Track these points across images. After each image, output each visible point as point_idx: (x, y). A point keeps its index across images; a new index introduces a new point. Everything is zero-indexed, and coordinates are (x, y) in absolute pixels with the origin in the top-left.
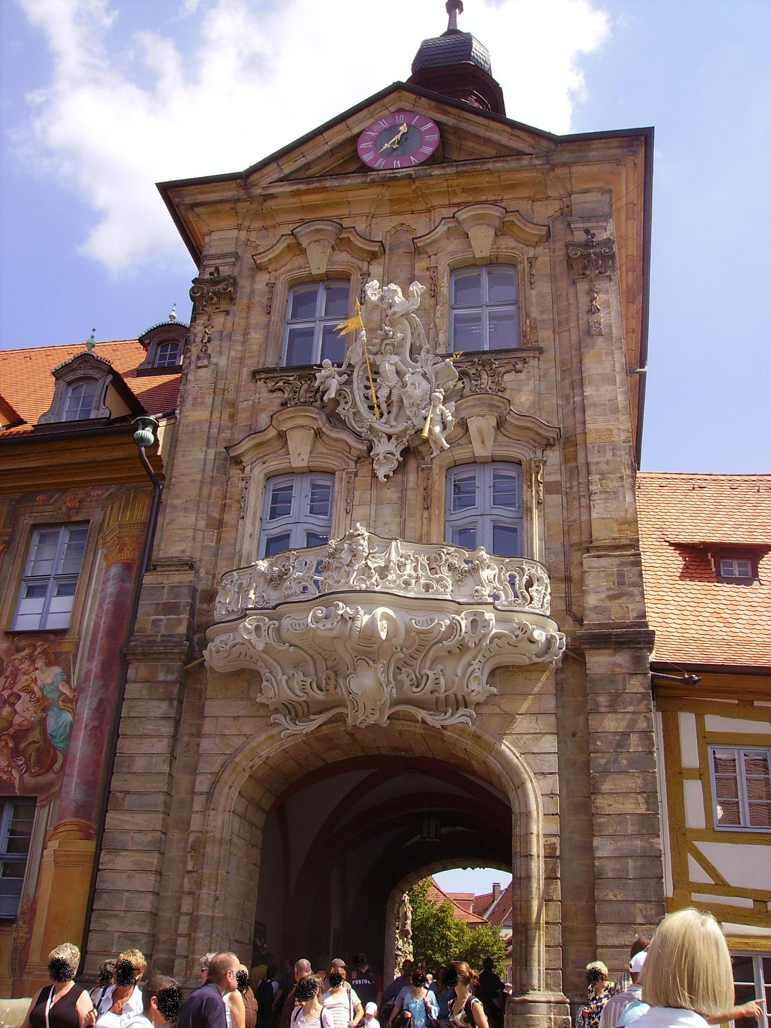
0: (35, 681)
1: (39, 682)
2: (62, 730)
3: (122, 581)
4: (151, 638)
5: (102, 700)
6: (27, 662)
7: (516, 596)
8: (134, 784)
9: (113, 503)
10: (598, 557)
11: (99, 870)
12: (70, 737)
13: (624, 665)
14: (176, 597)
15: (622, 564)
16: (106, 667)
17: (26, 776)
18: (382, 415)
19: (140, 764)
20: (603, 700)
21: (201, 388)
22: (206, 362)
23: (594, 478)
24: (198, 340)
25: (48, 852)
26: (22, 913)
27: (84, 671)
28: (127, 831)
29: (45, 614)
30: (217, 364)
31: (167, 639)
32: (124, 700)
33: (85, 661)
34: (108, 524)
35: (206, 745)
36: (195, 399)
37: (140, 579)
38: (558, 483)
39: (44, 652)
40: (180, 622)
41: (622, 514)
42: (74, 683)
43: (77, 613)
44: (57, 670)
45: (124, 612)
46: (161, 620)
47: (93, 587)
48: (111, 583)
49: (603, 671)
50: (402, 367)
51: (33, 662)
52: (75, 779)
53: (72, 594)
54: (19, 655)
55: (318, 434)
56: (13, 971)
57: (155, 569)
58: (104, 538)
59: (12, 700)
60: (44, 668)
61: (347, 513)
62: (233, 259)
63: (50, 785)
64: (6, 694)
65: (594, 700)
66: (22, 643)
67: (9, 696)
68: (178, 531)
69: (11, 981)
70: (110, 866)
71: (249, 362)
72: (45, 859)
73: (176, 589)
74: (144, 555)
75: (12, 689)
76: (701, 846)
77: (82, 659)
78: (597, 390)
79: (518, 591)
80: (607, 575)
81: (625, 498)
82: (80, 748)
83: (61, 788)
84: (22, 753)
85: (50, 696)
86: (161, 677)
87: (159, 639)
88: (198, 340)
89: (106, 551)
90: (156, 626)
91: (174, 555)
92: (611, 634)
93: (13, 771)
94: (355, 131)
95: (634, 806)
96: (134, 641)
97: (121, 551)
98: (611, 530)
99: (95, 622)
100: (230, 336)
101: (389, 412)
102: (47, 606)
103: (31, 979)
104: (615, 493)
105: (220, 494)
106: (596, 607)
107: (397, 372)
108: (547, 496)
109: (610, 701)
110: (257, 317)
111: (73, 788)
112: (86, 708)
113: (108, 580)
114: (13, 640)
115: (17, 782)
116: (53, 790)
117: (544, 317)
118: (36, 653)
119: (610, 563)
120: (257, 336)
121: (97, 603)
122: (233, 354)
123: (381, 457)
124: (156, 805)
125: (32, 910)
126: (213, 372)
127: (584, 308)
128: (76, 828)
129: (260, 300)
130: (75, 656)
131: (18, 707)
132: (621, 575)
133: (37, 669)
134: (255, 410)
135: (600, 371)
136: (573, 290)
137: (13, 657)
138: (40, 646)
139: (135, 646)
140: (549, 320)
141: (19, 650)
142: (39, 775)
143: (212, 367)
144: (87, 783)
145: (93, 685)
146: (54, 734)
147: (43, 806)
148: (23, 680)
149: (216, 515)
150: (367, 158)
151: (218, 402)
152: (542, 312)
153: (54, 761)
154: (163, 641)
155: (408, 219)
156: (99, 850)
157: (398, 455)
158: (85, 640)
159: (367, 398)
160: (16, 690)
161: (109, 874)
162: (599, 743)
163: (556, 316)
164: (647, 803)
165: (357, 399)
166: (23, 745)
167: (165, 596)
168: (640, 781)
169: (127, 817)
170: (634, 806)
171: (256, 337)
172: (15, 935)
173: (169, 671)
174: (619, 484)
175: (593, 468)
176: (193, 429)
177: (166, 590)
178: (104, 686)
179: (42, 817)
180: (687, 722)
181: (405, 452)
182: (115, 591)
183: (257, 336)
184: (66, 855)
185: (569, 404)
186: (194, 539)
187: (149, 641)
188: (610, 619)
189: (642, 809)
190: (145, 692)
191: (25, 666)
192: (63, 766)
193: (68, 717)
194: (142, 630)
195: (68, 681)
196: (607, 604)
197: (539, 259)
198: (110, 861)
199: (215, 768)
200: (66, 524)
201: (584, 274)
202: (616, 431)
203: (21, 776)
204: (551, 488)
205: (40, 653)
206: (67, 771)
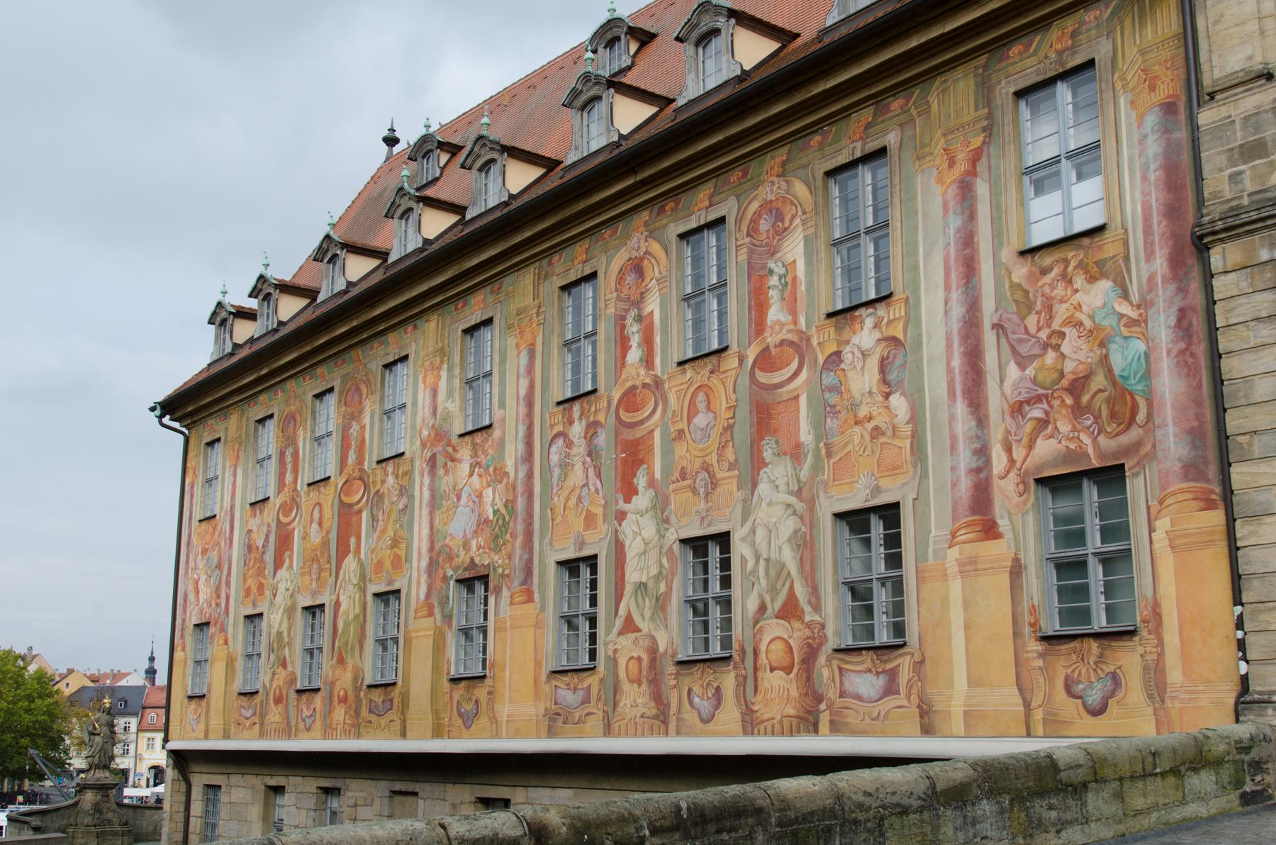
0: (1079, 307)
1: (1085, 308)
4: (1234, 204)
5: (1182, 313)
6: (1061, 286)
11: (1238, 549)
12: (1148, 374)
14: (1257, 130)
16: (1176, 262)
17: (1102, 439)
25: (1159, 535)
26: (1144, 621)
27: (1144, 280)
29: (1067, 211)
32: (1215, 302)
33: (1143, 263)
37: (1192, 119)
39: (1081, 266)
42: (1135, 297)
43: (1111, 197)
44: (1105, 285)
45: (1184, 174)
46: (1241, 173)
51: (1070, 282)
53: (1098, 173)
54: (1048, 279)
56: (1150, 697)
57: (1212, 98)
59: (1054, 341)
60: (1087, 286)
63: (1137, 445)
64: (1043, 335)
66: (1047, 259)
67: (1049, 337)
69: (1150, 710)
72: (1156, 546)
73: (1253, 119)
74: (1188, 80)
75: (1049, 326)
77: (1137, 260)
82: (1169, 385)
83: (1154, 446)
84: (1088, 408)
85: (1106, 323)
90: (1236, 183)
93: (1083, 437)
96: (1208, 214)
99: (1143, 203)
102: (1067, 199)
103: (1177, 705)
111: (1172, 443)
114: (1033, 261)
115: (1091, 451)
116: (1144, 451)
118: (1070, 269)
121: (1138, 175)
125: (1157, 614)
128: (1189, 496)
130: (1127, 258)
131: (1065, 348)
133: (1076, 291)
137: (1040, 284)
138: (1072, 255)
141: (1044, 272)
142: (1117, 435)
144: (1191, 432)
146: (1125, 374)
147: (1135, 475)
148: (1062, 312)
153: (1134, 410)
154: (1251, 204)
156: (1231, 520)
158: (1134, 233)
160: (1055, 326)
166: (1085, 399)
167: (1239, 134)
172: (1140, 650)
177: (1238, 126)
179: (1137, 489)
182: (1160, 150)
186: (1262, 33)
187: (1232, 209)
191: (1059, 291)
192: (1149, 417)
193: (1140, 346)
194: (1215, 195)
195: (1125, 296)
200: (1064, 76)
203: (1094, 440)
205: (1075, 268)
206: (1158, 421)
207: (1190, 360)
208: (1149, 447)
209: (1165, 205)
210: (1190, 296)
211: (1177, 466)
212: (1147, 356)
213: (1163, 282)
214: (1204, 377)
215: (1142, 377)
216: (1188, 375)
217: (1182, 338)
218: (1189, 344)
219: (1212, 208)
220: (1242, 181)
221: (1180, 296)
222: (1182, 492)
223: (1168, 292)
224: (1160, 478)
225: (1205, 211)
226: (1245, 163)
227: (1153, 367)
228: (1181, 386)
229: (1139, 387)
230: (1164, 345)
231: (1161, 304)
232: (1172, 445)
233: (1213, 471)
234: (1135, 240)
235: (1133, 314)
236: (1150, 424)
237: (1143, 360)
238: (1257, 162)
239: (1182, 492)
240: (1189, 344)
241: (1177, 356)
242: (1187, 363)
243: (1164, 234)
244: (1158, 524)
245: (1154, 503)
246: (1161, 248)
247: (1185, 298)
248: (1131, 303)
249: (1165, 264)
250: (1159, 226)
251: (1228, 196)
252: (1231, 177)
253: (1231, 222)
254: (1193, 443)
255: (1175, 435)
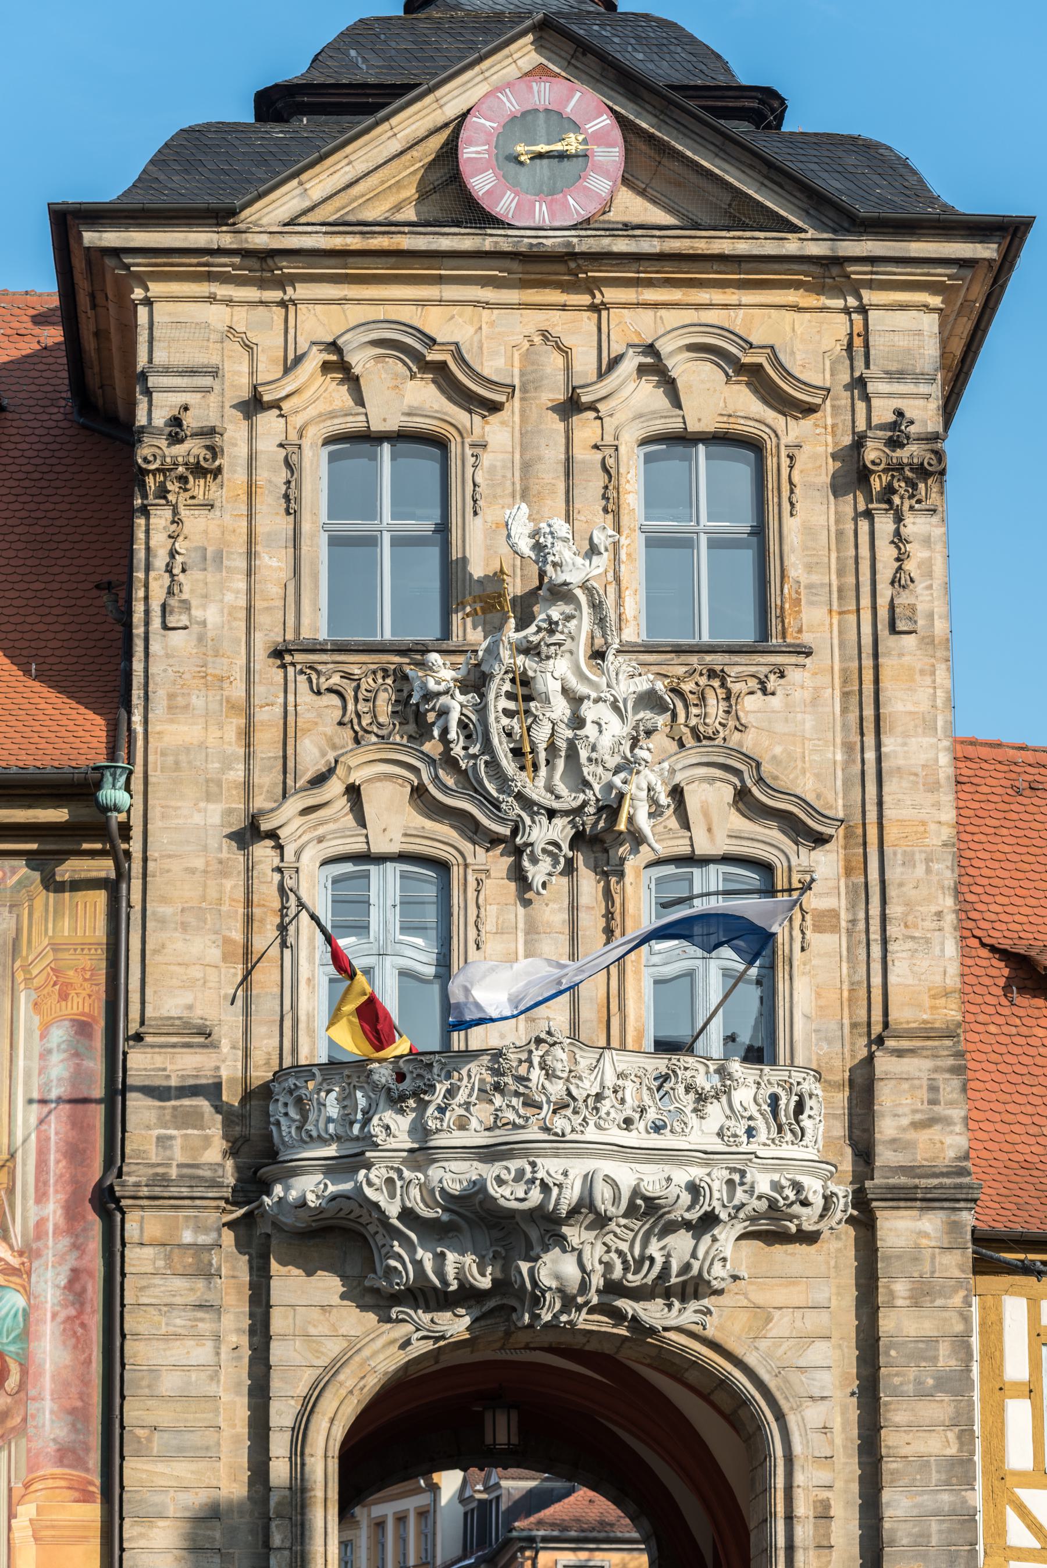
2: (9, 1321)
3: (77, 1054)
5: (76, 1273)
7: (780, 1129)
8: (163, 1415)
9: (31, 899)
10: (900, 1053)
12: (25, 1335)
13: (933, 1234)
15: (936, 1070)
16: (71, 1213)
18: (536, 767)
19: (169, 1383)
20: (901, 1288)
21: (181, 675)
22: (184, 620)
23: (894, 910)
24: (160, 561)
28: (164, 1489)
30: (204, 623)
31: (191, 1175)
34: (29, 942)
35: (278, 1352)
36: (171, 696)
38: (834, 914)
40: (207, 1140)
41: (938, 979)
42: (17, 1241)
46: (171, 1138)
47: (21, 1063)
48: (55, 1058)
49: (901, 1242)
50: (573, 682)
52: (48, 1404)
55: (419, 792)
58: (25, 969)
61: (478, 948)
62: (207, 381)
65: (888, 1287)
68: (177, 969)
70: (142, 1543)
71: (261, 619)
72: (16, 1534)
76: (1025, 1495)
77: (24, 1197)
78: (905, 744)
79: (784, 1120)
80: (913, 1088)
81: (943, 950)
83: (25, 1420)
86: (188, 1237)
87: (174, 1173)
88: (160, 561)
89: (34, 996)
90: (165, 1148)
91: (174, 1013)
92: (916, 1187)
94: (452, 110)
95: (941, 1445)
96: (129, 1174)
97: (64, 996)
98: (919, 1006)
100: (219, 558)
101: (548, 762)
104: (928, 941)
105: (240, 894)
106: (894, 1141)
107: (565, 691)
108: (817, 935)
109: (911, 1290)
110: (272, 521)
112: (49, 1284)
113: (49, 1051)
117: (815, 578)
119: (916, 1067)
120: (274, 563)
122: (229, 597)
123: (538, 850)
124: (207, 1448)
126: (201, 639)
127: (885, 573)
128: (63, 1483)
129: (271, 477)
132: (933, 1089)
134: (288, 733)
135: (910, 708)
136: (864, 525)
139: (137, 1185)
140: (822, 585)
143: (195, 629)
144: (73, 1412)
145: (54, 1246)
149: (237, 935)
150: (481, 184)
151: (214, 706)
152: (809, 568)
154: (181, 1176)
155: (556, 322)
157: (565, 847)
158: (24, 1164)
159: (509, 735)
161: (143, 1556)
162: (893, 1353)
163: (834, 577)
164: (961, 1444)
165: (495, 741)
168: (950, 1410)
169: (160, 1467)
170: (941, 1445)
171: (274, 563)
173: (198, 1229)
174: (934, 925)
175: (892, 892)
176: (177, 763)
178: (75, 1246)
180: (1015, 1310)
181: (578, 840)
182: (66, 1074)
183: (274, 563)
184: (53, 1527)
185: (854, 761)
188: (914, 1160)
189: (953, 1450)
190: (161, 1263)
192: (22, 1386)
193: (20, 1301)
194: (139, 1153)
196: (911, 1135)
197: (806, 448)
198: (142, 1536)
199: (302, 1389)
201: (889, 502)
202: (933, 827)
204: (827, 921)
206: (32, 1393)
207: (80, 1331)
208: (19, 1420)
209: (67, 1143)
210: (87, 1258)
211: (52, 1448)
212: (26, 1314)
213: (54, 1233)
214: (95, 1354)
215: (18, 1336)
216: (75, 1347)
217: (73, 1304)
218: (80, 1313)
219: (133, 1168)
220: (171, 1147)
221: (75, 1254)
222: (54, 1477)
223: (60, 1246)
224: (28, 1458)
225: (125, 1169)
226: (177, 1128)
227: (32, 1329)
228: (65, 1357)
229: (12, 1348)
230: (49, 1306)
231: (51, 1258)
232: (47, 1423)
233: (94, 1459)
234: (24, 1173)
235: (15, 1261)
236: (22, 1395)
237: (20, 1318)
238: (190, 1131)
239: (54, 1477)
240: (80, 1313)
241: (64, 1322)
242: (75, 1333)
243: (61, 1176)
244: (21, 1510)
245: (17, 1486)
246: (56, 1192)
247: (80, 1258)
248: (11, 1247)
249: (59, 1212)
250: (56, 1164)
251: (154, 1160)
252: (160, 1139)
253: (157, 1191)
254: (74, 1425)
255: (52, 1412)
